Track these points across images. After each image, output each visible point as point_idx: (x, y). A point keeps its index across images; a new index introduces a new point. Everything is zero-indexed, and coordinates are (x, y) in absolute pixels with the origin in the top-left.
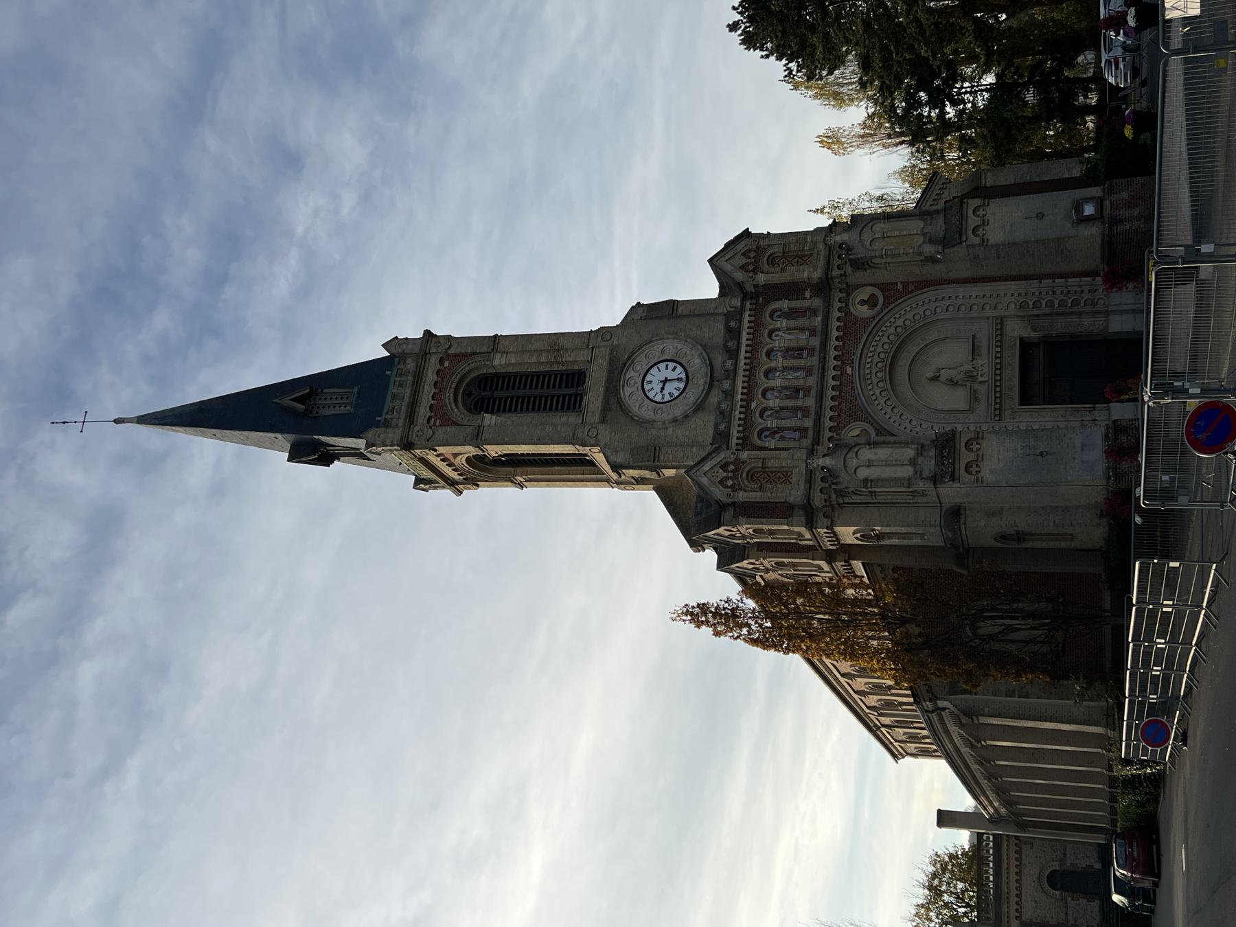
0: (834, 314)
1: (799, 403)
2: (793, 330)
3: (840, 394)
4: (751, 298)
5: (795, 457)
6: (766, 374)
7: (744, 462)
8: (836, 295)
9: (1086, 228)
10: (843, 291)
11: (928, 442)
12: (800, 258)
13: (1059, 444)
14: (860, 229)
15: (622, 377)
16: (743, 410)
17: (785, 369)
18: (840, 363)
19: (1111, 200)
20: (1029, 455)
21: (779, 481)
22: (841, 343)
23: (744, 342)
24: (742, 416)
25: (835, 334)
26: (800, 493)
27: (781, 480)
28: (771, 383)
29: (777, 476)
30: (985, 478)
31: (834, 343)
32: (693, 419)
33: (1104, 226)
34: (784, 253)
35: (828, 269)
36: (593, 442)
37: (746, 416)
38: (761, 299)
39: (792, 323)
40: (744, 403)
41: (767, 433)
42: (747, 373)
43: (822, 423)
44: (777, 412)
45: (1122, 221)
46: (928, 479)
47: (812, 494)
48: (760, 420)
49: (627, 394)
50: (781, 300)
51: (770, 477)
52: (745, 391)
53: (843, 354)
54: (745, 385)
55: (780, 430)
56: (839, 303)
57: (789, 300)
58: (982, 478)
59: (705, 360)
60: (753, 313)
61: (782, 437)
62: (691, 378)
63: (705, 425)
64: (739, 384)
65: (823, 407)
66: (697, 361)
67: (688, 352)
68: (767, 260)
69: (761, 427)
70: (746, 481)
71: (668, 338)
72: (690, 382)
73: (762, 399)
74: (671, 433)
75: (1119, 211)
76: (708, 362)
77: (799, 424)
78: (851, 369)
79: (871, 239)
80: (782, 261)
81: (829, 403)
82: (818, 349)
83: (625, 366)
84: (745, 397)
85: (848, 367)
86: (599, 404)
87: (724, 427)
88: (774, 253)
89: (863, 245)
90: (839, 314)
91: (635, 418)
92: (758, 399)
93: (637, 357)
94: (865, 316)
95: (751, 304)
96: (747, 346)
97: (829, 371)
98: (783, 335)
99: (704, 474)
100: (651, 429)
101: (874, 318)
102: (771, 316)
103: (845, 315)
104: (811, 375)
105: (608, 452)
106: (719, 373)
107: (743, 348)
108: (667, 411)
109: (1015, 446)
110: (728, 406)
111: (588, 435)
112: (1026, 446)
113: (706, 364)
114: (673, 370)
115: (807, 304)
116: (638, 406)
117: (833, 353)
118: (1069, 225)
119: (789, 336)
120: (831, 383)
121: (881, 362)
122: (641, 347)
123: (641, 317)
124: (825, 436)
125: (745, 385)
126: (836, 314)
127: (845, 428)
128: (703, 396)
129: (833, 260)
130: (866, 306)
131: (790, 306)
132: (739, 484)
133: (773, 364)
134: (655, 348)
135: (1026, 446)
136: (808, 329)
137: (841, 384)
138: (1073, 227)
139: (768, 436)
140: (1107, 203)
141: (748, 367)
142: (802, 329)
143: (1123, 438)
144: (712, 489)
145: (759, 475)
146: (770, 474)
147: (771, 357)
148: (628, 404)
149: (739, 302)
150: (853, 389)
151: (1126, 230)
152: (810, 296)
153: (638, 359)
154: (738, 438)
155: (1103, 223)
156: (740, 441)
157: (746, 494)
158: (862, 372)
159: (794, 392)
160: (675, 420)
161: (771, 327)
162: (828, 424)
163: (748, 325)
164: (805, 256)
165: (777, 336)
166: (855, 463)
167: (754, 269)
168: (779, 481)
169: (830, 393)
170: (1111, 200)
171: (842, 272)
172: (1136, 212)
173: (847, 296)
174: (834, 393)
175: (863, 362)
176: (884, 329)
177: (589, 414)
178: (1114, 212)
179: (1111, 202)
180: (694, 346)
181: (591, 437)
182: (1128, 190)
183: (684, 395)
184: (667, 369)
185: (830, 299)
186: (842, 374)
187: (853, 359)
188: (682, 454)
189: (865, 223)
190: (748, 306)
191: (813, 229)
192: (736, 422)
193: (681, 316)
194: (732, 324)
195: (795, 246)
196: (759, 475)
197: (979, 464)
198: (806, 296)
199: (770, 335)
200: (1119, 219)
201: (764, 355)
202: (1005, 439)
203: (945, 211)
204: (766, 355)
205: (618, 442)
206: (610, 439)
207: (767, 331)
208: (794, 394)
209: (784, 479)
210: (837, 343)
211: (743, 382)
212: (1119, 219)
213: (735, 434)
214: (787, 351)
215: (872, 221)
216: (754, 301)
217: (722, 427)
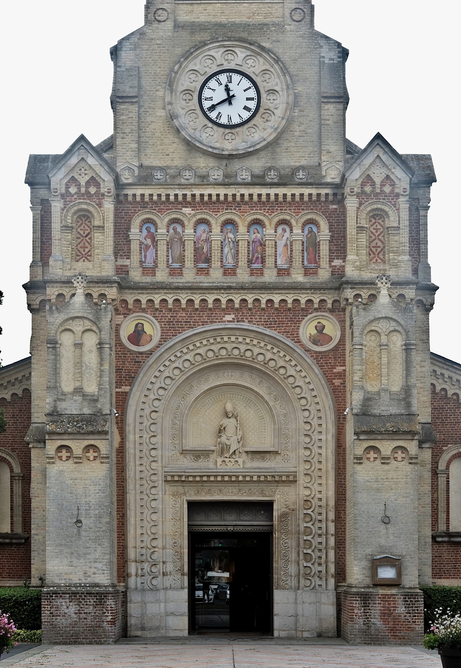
0: (303, 296)
1: (189, 263)
2: (291, 248)
3: (197, 309)
4: (335, 195)
5: (104, 263)
6: (229, 222)
7: (100, 205)
8: (330, 296)
9: (365, 568)
10: (336, 304)
11: (99, 406)
12: (382, 250)
13: (90, 539)
14: (394, 317)
15: (235, 43)
16: (180, 198)
17: (236, 243)
18: (237, 306)
19: (397, 595)
20: (78, 509)
21: (81, 247)
22: (263, 306)
23: (272, 191)
24: (172, 198)
25: (277, 298)
26: (59, 272)
27: (82, 250)
28: (216, 229)
29: (87, 244)
30: (55, 465)
31: (264, 298)
32: (177, 140)
33: (362, 588)
34: (388, 228)
35: (354, 284)
36: (151, 16)
37: (172, 203)
38: (334, 207)
39: (297, 247)
40: (189, 198)
41: (153, 230)
42: (230, 199)
43: (157, 291)
44: (181, 239)
45: (366, 605)
46: (55, 407)
47: (55, 285)
48: (166, 220)
49: (212, 53)
50: (330, 232)
51: (86, 236)
52: (206, 198)
53: (250, 309)
54: (214, 198)
55: (155, 242)
56: (318, 300)
57: (330, 242)
58: (53, 463)
59: (254, 146)
60: (314, 198)
61: (147, 247)
62: (233, 131)
63: (168, 155)
64: (214, 192)
65: (179, 291)
66: (256, 137)
67: (269, 124)
68: (377, 209)
69: (158, 222)
70: (76, 208)
71: (288, 96)
72: (227, 131)
73: (195, 219)
74: (158, 114)
75: (379, 603)
76: (252, 149)
77: (162, 265)
78: (231, 319)
79: (380, 331)
80: (379, 227)
81: (184, 297)
82: (260, 280)
83: (251, 44)
84: (198, 198)
85: (233, 316)
86: (203, 18)
87: (159, 177)
88: (388, 216)
89: (372, 321)
90: (303, 301)
91: (176, 68)
92: (194, 215)
93: (265, 58)
94: (301, 331)
95: (327, 195)
96: (277, 195)
97: (226, 295)
98: (285, 238)
99: (83, 159)
100: (165, 88)
101: (299, 342)
102: (311, 222)
103: (303, 309)
104: (225, 274)
105: (134, 39)
106: (236, 165)
107: (264, 191)
108: (188, 106)
109: (90, 496)
110: (187, 179)
111: (158, 9)
112: (90, 507)
113: (250, 147)
114: (246, 108)
115: (324, 262)
116: (196, 68)
117: (250, 298)
118: (369, 551)
119: (283, 244)
120: (211, 299)
121: (240, 352)
122: (277, 62)
123: (323, 57)
124: (142, 295)
125: (214, 198)
126: (303, 299)
127: (153, 317)
128: (205, 148)
129: (369, 289)
130: (314, 332)
131: (321, 243)
132: (71, 202)
133: (242, 229)
134: (278, 80)
135: (90, 507)
136: (291, 266)
137: (210, 309)
138: (366, 555)
139: (149, 231)
140: (394, 591)
141: (238, 198)
142: (290, 260)
143: (92, 601)
144: (63, 170)
145: (89, 224)
146: (89, 236)
147: (252, 229)
148: (198, 56)
149: (333, 180)
150: (204, 323)
151: (354, 610)
152: (336, 266)
153: (261, 60)
154: (143, 195)
155: (368, 587)
156: (138, 199)
157: (58, 209)
158: (224, 333)
159: (206, 258)
160: (172, 117)
161: (293, 222)
162: (157, 298)
163: (297, 194)
164: (384, 255)
165: (284, 230)
166: (77, 329)
167: (366, 193)
168: (81, 247)
169: (197, 299)
170: (397, 595)
171: (350, 301)
172: (377, 622)
173: (328, 309)
174: (197, 302)
175: (238, 333)
176: (282, 354)
177: (190, 8)
178: (379, 598)
179: (394, 595)
180: (276, 129)
181: (155, 13)
182: (407, 613)
183: (210, 125)
184: (248, 99)
185: (324, 289)
186: (223, 310)
187: (244, 321)
188: (127, 131)
189: (402, 322)
190: (324, 191)
191: (429, 262)
192: (163, 192)
193: (320, 109)
194: (301, 175)
195: (396, 241)
196: (89, 224)
197: (71, 459)
198: (335, 261)
199: (283, 222)
200: (369, 603)
201: (255, 217)
202: (100, 485)
203: (407, 415)
204: (255, 219)
205: (148, 50)
206: (152, 39)
207: (288, 218)
208: (203, 257)
209: (84, 253)
210: (263, 301)
211: (218, 195)
212: (369, 603)
213: (147, 192)
214: (261, 245)
215: (405, 330)
216: (331, 198)
217: (158, 175)
